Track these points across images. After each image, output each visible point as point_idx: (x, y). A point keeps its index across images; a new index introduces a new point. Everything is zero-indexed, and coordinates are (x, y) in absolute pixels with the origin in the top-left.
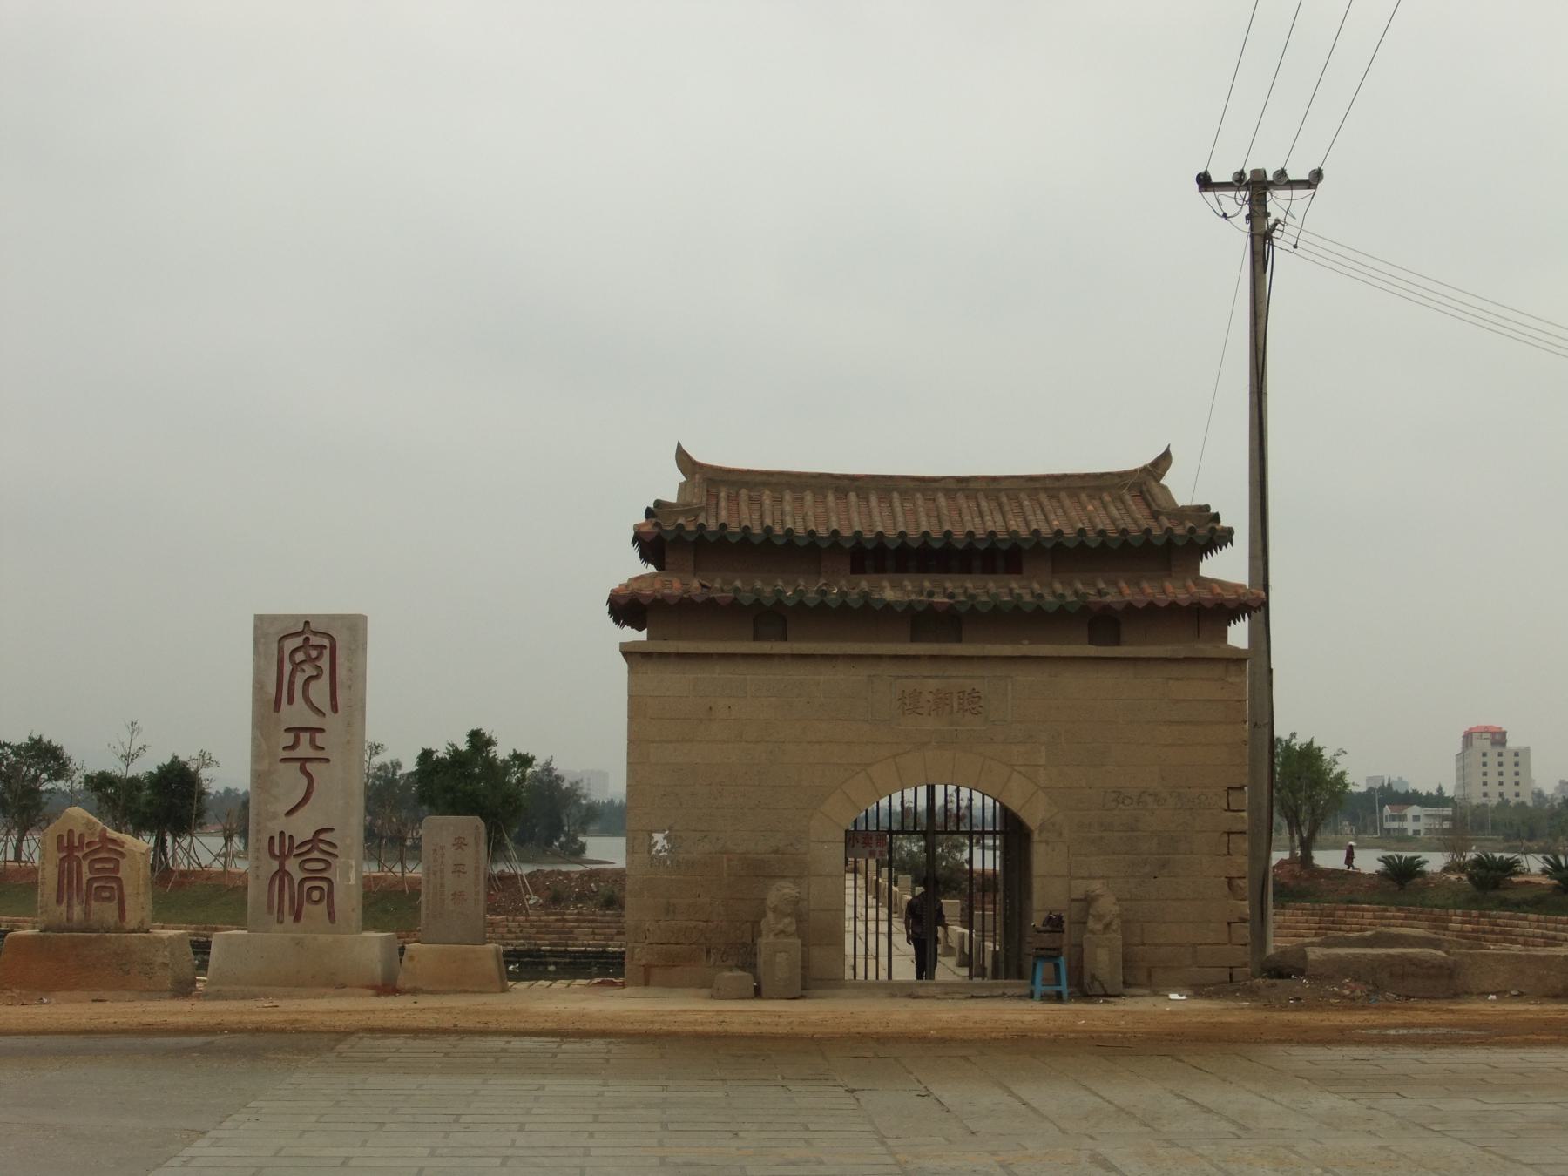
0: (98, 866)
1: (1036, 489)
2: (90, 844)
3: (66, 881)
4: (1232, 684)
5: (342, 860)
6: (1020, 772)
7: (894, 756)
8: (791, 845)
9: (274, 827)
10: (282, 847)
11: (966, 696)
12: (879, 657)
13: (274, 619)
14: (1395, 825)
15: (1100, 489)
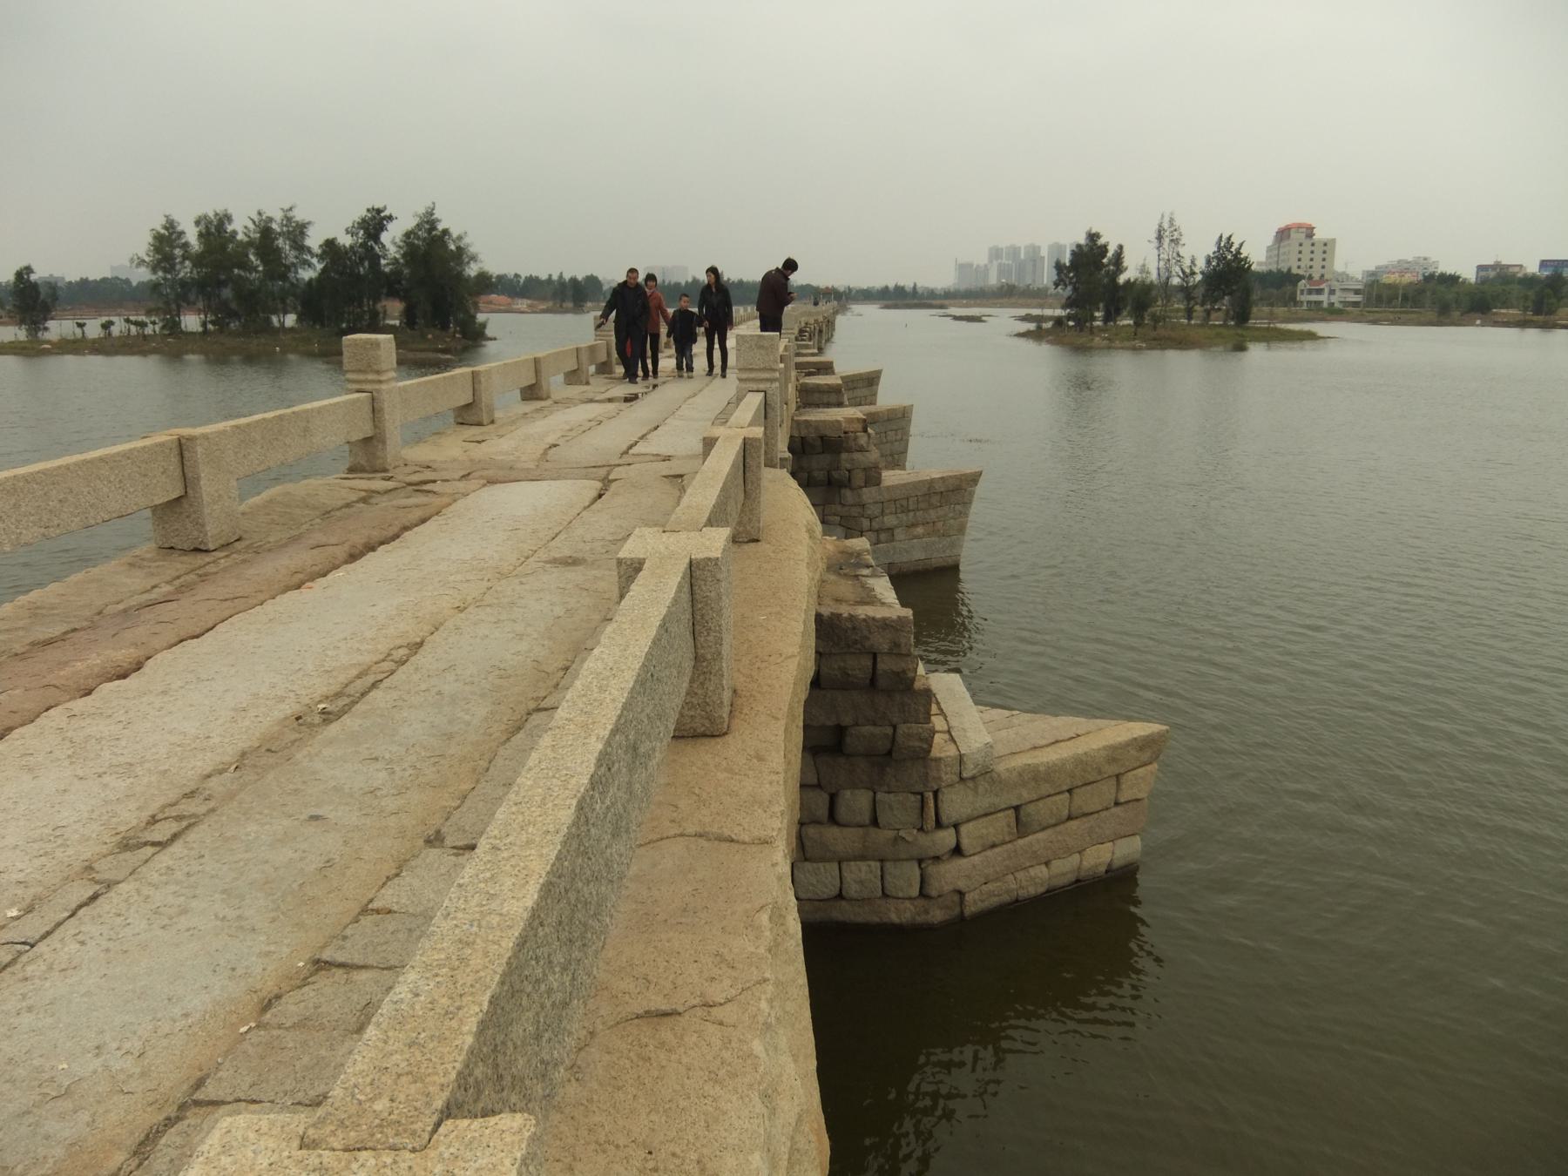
14: (1314, 298)
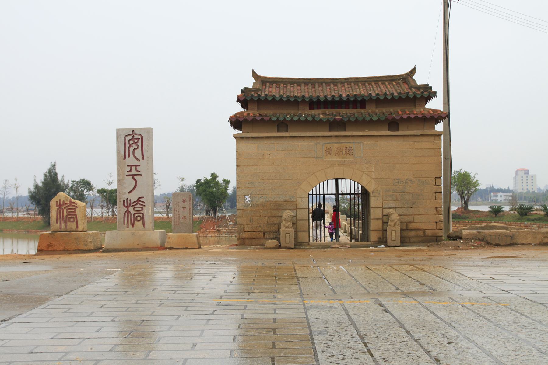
0: (69, 211)
1: (371, 81)
2: (66, 204)
3: (59, 216)
4: (437, 143)
5: (147, 207)
6: (366, 174)
7: (324, 169)
8: (290, 199)
9: (125, 197)
10: (128, 204)
11: (348, 149)
12: (319, 137)
13: (123, 130)
14: (495, 198)
15: (392, 80)
